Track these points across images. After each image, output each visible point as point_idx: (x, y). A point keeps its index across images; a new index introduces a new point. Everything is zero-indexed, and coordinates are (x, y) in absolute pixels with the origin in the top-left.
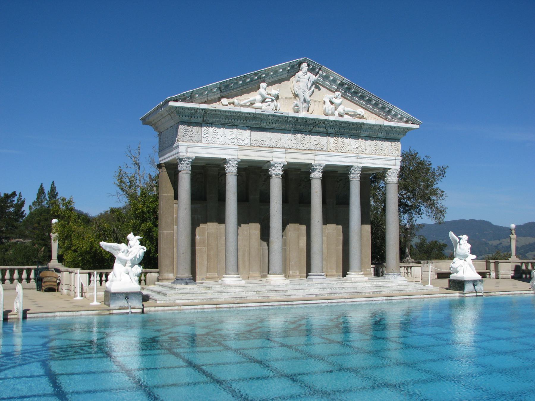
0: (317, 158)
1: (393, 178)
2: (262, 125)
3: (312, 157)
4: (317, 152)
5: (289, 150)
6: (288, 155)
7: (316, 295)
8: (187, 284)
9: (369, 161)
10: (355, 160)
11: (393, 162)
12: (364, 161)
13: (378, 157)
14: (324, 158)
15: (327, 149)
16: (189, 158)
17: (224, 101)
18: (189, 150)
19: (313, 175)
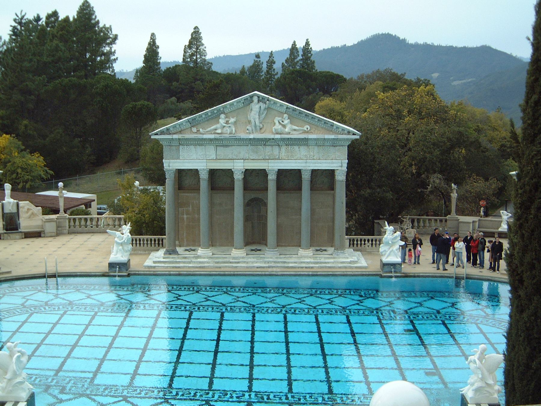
0: (270, 165)
1: (341, 177)
2: (225, 143)
3: (267, 164)
4: (269, 161)
5: (246, 161)
6: (246, 164)
7: (257, 268)
8: (170, 254)
9: (317, 165)
10: (304, 165)
11: (340, 165)
12: (311, 165)
13: (325, 161)
14: (276, 165)
15: (279, 157)
16: (171, 170)
17: (194, 130)
18: (171, 165)
19: (270, 177)
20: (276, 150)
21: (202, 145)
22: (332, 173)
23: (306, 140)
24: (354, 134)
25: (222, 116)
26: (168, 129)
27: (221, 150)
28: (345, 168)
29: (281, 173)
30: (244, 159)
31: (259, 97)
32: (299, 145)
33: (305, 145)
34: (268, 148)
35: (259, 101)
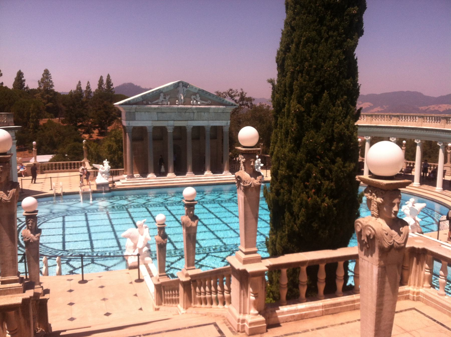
20: (192, 115)
21: (149, 112)
22: (221, 128)
23: (209, 109)
24: (235, 105)
25: (162, 95)
26: (129, 101)
27: (159, 114)
28: (229, 124)
29: (194, 128)
30: (174, 121)
31: (183, 83)
32: (205, 112)
33: (207, 112)
34: (187, 114)
35: (183, 86)
